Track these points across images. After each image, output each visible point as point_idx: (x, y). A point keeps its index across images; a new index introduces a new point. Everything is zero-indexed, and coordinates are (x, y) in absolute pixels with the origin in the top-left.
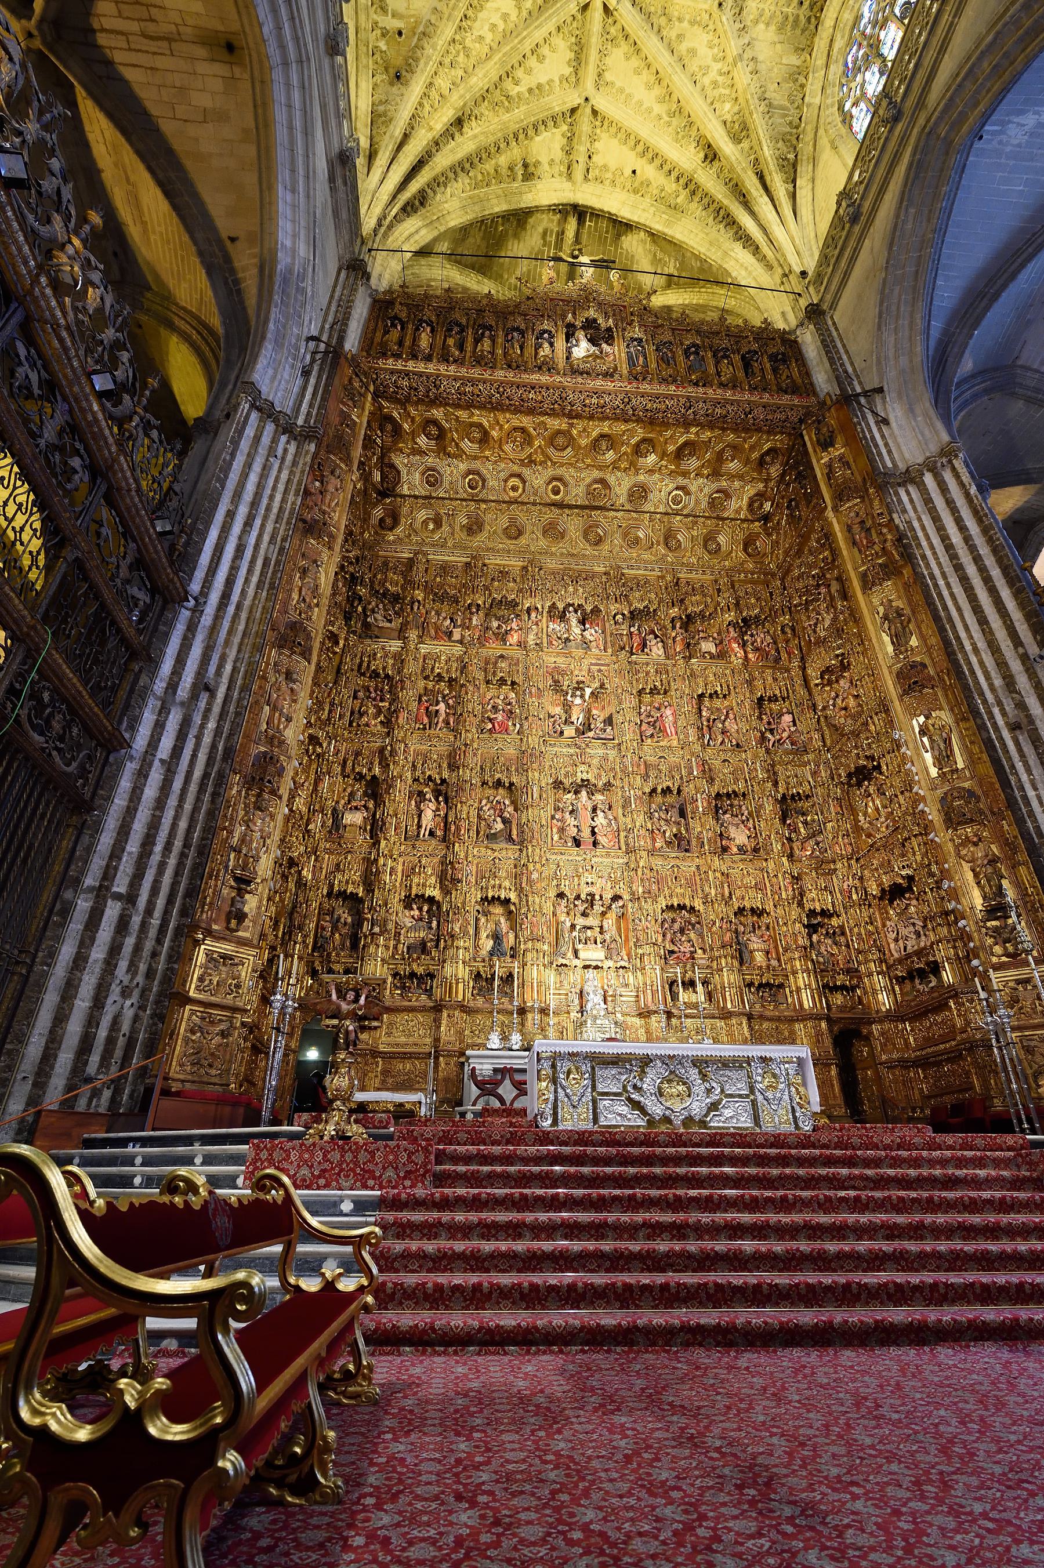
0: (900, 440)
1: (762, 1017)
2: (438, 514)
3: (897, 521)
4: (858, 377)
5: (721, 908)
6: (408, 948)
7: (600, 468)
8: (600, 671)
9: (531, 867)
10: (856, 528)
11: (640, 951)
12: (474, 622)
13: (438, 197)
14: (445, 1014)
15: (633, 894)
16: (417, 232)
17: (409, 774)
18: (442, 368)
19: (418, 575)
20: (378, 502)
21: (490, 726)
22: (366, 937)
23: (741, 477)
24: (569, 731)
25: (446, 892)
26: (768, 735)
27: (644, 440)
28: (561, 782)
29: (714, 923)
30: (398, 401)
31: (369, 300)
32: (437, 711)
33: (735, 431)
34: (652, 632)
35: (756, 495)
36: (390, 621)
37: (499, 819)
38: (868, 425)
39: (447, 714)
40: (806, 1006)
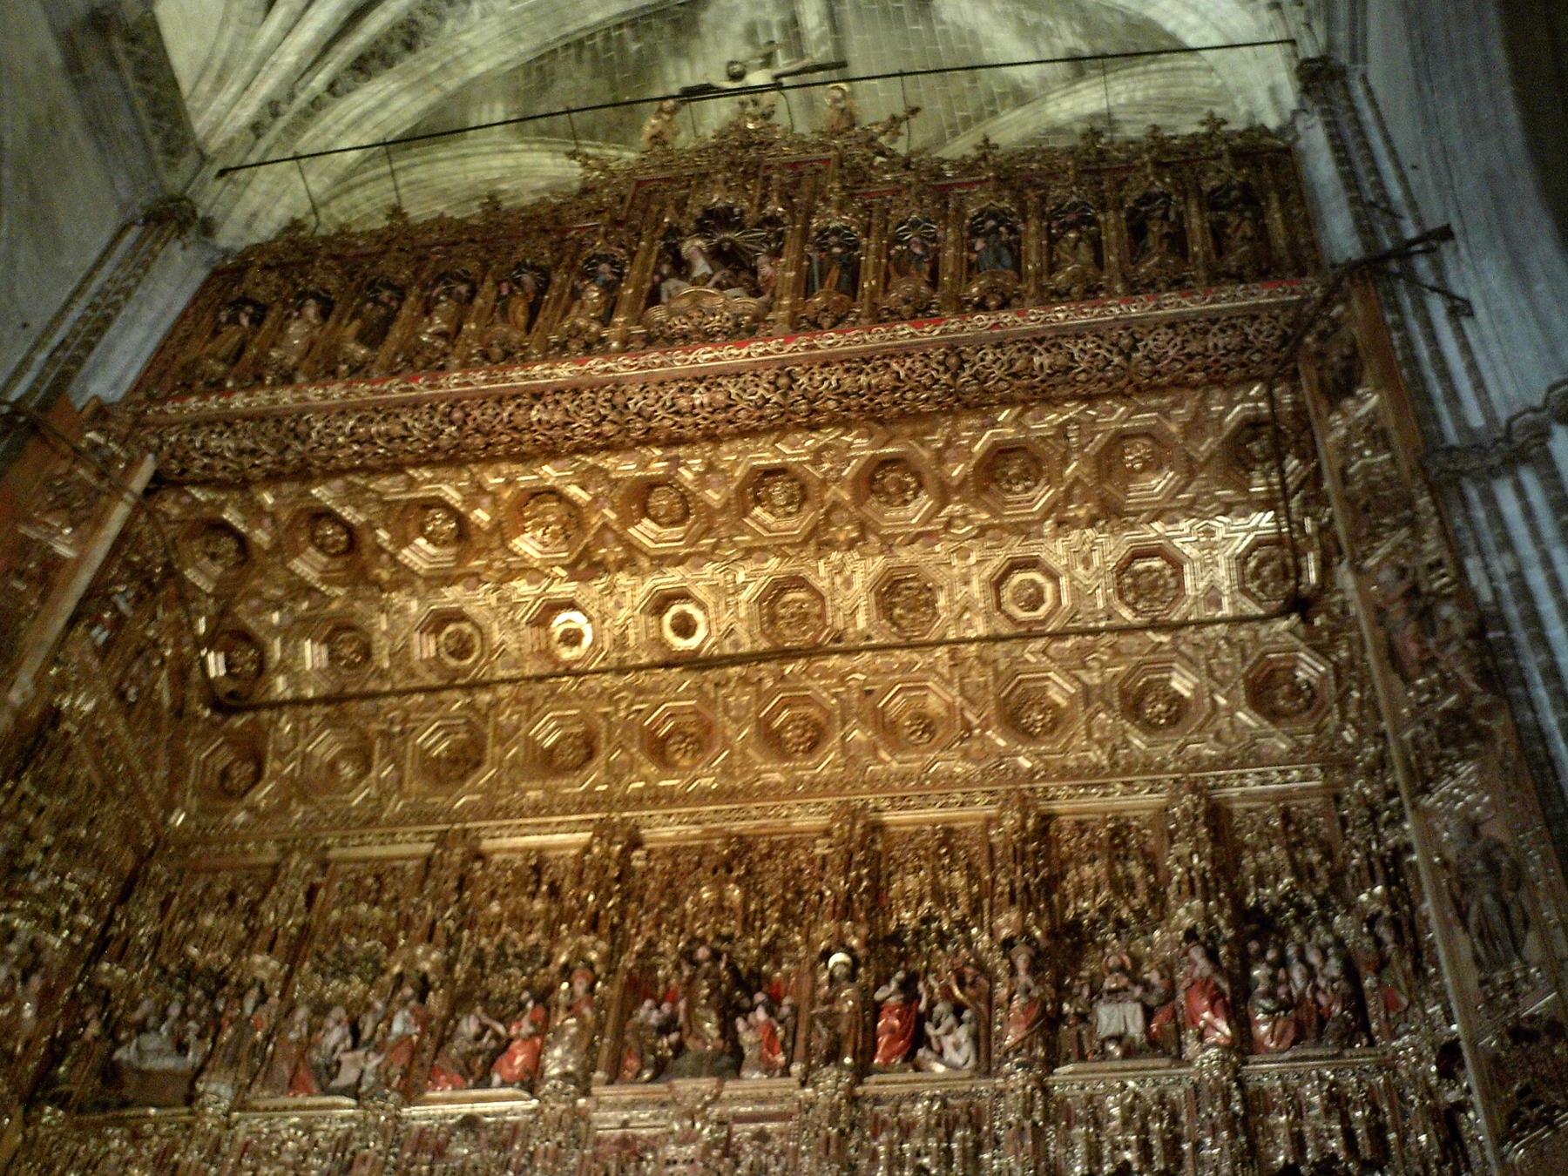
0: (1494, 350)
2: (364, 737)
3: (1476, 577)
4: (1413, 205)
7: (779, 550)
10: (1397, 612)
12: (397, 1027)
13: (450, 25)
16: (383, 104)
18: (313, 394)
19: (278, 915)
20: (215, 726)
23: (1189, 509)
27: (885, 463)
30: (222, 486)
31: (201, 274)
33: (1121, 395)
34: (947, 993)
35: (1257, 544)
36: (181, 1048)
38: (1428, 324)
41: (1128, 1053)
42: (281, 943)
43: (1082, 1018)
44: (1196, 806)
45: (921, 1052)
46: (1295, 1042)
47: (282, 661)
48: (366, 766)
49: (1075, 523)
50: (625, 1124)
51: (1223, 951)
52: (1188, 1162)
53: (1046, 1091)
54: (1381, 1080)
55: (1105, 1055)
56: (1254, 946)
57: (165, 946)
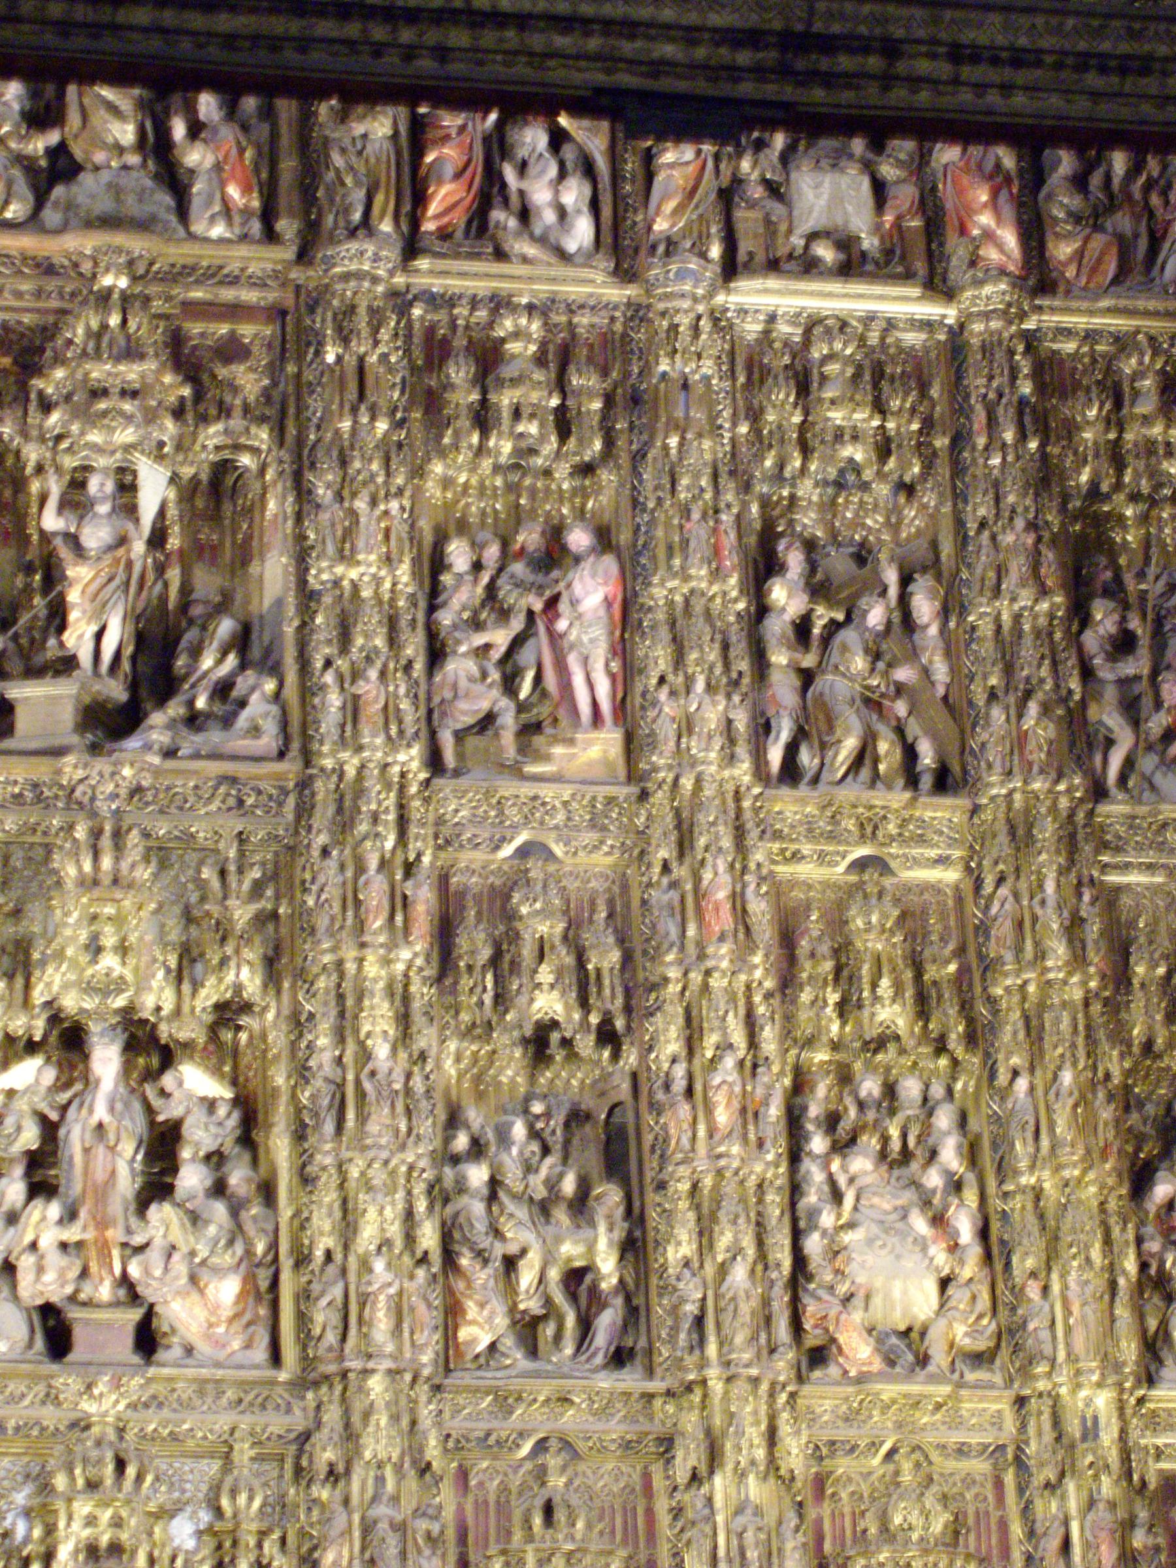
43: (774, 190)
45: (498, 215)
46: (1116, 281)
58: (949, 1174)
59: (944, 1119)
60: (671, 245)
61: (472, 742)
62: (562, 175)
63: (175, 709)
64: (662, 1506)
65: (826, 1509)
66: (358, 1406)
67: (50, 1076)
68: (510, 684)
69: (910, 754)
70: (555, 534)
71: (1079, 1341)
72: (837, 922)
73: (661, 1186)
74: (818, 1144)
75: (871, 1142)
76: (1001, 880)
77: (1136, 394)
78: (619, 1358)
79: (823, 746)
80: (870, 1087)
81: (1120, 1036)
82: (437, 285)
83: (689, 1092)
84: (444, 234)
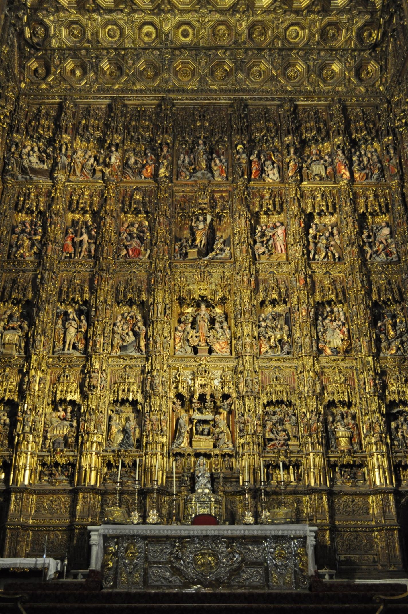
1: (341, 493)
5: (312, 403)
6: (54, 443)
8: (222, 197)
9: (155, 373)
11: (242, 441)
12: (113, 160)
14: (81, 496)
15: (238, 392)
17: (56, 298)
21: (125, 252)
22: (19, 435)
24: (193, 253)
25: (84, 396)
26: (367, 248)
28: (184, 299)
29: (305, 415)
32: (81, 241)
36: (43, 162)
37: (131, 333)
39: (89, 243)
40: (378, 483)
41: (321, 180)
42: (69, 131)
44: (339, 107)
45: (263, 175)
47: (55, 34)
48: (85, 73)
49: (313, 12)
50: (183, 192)
51: (346, 152)
52: (338, 210)
53: (300, 188)
54: (387, 191)
55: (315, 179)
56: (353, 150)
57: (31, 129)
58: (342, 322)
59: (341, 314)
60: (292, 177)
61: (262, 256)
62: (274, 167)
63: (214, 253)
64: (296, 377)
65: (323, 377)
66: (245, 361)
67: (194, 310)
68: (267, 247)
69: (334, 255)
70: (275, 224)
71: (366, 349)
72: (321, 282)
73: (294, 325)
74: (320, 318)
75: (329, 318)
76: (350, 274)
77: (370, 197)
78: (288, 353)
79: (319, 255)
80: (329, 309)
81: (371, 299)
82: (254, 186)
83: (298, 310)
84: (255, 178)
